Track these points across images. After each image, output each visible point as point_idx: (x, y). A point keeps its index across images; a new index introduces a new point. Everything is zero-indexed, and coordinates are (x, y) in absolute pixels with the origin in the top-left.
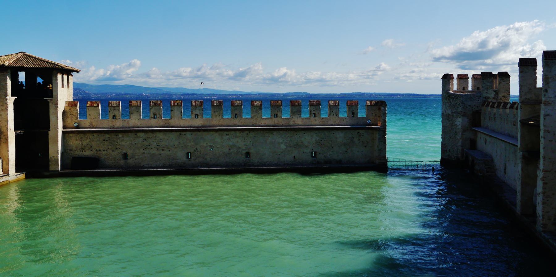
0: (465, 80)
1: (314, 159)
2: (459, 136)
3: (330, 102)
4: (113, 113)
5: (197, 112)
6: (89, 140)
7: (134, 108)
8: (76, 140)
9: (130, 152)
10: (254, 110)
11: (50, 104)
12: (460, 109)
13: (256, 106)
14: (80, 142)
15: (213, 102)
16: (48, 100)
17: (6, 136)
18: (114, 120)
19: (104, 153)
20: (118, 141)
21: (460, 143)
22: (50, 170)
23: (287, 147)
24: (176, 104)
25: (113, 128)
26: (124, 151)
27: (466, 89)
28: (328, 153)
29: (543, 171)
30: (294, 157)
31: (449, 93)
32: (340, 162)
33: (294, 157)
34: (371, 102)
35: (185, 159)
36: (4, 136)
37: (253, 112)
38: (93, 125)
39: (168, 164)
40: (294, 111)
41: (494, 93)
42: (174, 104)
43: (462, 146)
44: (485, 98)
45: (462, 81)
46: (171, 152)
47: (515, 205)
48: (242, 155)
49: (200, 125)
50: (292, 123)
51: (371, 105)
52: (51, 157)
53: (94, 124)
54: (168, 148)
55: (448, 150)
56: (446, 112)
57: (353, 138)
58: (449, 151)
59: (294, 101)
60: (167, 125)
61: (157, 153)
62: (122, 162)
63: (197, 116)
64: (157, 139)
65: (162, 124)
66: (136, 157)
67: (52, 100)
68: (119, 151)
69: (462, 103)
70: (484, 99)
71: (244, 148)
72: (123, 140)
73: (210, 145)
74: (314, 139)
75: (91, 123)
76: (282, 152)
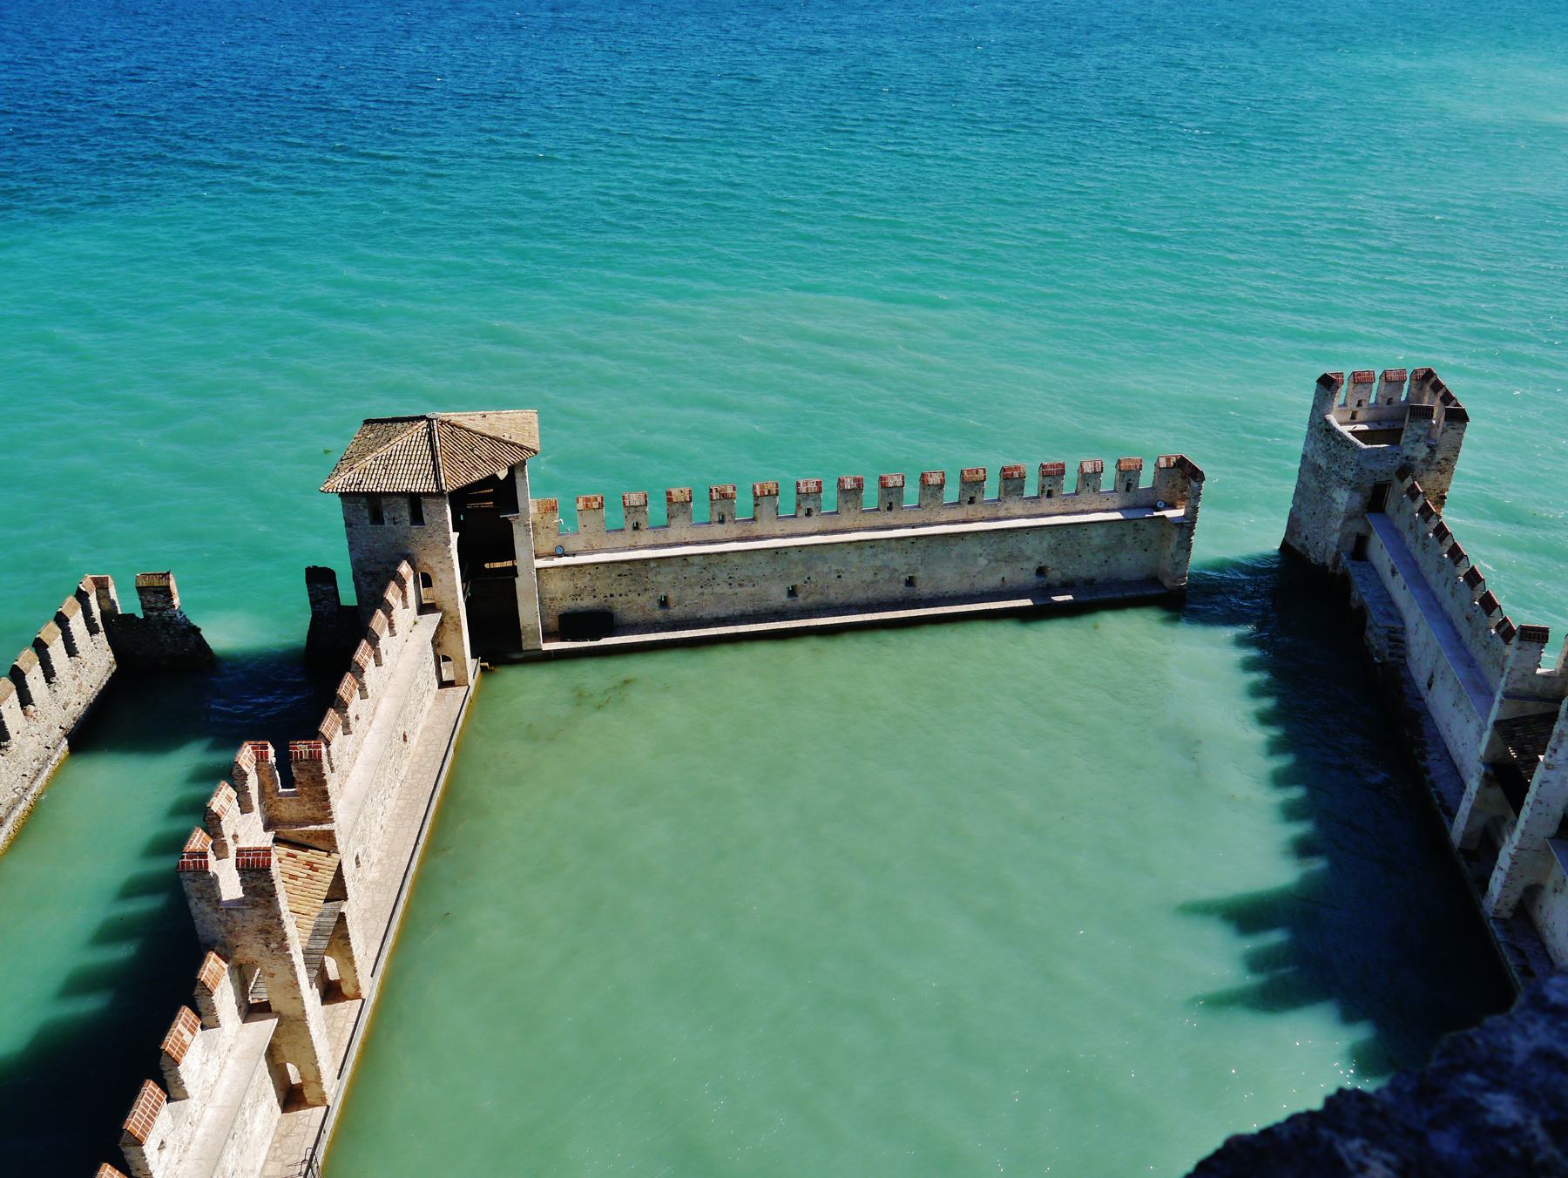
0: (1366, 385)
1: (1040, 580)
2: (1337, 524)
4: (633, 518)
5: (810, 504)
6: (589, 577)
7: (677, 505)
8: (562, 579)
9: (673, 596)
10: (929, 492)
11: (514, 526)
12: (1349, 474)
13: (933, 485)
14: (571, 583)
15: (843, 481)
17: (456, 619)
18: (636, 532)
19: (620, 599)
20: (650, 576)
21: (1335, 537)
23: (990, 561)
24: (766, 493)
25: (634, 548)
26: (663, 593)
27: (1363, 403)
28: (1071, 567)
29: (1515, 848)
31: (1327, 422)
32: (1090, 582)
34: (1168, 460)
35: (784, 598)
36: (452, 618)
37: (922, 495)
38: (591, 545)
39: (751, 609)
40: (1009, 489)
42: (762, 492)
43: (1338, 547)
44: (1407, 458)
45: (1360, 387)
46: (756, 587)
47: (1452, 815)
48: (899, 582)
49: (816, 530)
50: (1002, 513)
52: (524, 627)
53: (594, 543)
54: (750, 580)
55: (1303, 534)
56: (1313, 456)
57: (1124, 535)
58: (1307, 539)
59: (1010, 469)
60: (746, 534)
61: (730, 591)
62: (659, 614)
63: (809, 513)
64: (730, 565)
65: (736, 532)
66: (687, 603)
67: (517, 518)
68: (651, 594)
70: (1404, 461)
71: (904, 569)
72: (656, 575)
73: (836, 568)
74: (1045, 544)
75: (588, 542)
76: (979, 572)
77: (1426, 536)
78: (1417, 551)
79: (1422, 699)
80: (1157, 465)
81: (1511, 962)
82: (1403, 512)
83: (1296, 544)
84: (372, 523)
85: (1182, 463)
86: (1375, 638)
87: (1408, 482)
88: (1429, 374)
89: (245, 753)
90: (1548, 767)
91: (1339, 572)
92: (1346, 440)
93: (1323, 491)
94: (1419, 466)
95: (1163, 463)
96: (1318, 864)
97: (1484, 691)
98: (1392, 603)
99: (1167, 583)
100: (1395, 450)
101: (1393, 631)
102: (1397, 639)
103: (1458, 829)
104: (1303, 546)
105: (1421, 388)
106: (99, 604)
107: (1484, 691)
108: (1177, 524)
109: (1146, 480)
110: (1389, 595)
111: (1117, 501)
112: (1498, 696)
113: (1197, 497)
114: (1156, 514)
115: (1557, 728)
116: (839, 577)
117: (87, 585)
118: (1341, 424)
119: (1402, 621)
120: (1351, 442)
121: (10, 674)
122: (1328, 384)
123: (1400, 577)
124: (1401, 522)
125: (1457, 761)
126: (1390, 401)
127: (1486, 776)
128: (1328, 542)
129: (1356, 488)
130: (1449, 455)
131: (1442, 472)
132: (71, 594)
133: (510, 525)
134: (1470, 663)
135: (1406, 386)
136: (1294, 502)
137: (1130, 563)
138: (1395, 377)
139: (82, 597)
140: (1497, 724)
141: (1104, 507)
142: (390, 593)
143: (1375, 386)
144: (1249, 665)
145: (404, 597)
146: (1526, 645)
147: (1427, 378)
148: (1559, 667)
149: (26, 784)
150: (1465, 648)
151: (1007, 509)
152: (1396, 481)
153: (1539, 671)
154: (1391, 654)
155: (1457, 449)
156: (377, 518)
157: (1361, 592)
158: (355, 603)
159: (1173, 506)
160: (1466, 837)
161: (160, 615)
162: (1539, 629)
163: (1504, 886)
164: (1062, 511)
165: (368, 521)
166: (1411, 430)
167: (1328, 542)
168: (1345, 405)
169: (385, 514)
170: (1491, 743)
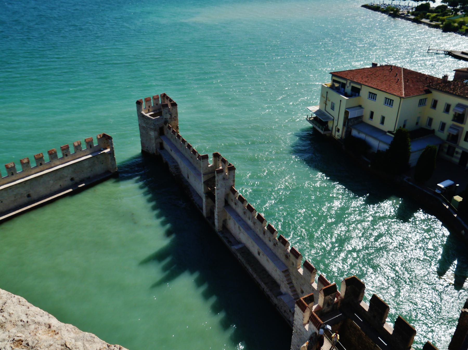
2: (153, 141)
3: (75, 144)
12: (152, 127)
21: (154, 145)
30: (60, 185)
31: (142, 114)
32: (89, 178)
33: (60, 185)
34: (100, 135)
37: (23, 167)
41: (170, 115)
44: (165, 119)
45: (148, 102)
47: (202, 209)
50: (53, 165)
51: (101, 138)
55: (146, 146)
57: (94, 161)
59: (50, 151)
69: (153, 124)
77: (176, 138)
78: (174, 143)
79: (188, 182)
80: (97, 138)
81: (225, 241)
82: (168, 134)
83: (145, 150)
85: (104, 135)
86: (172, 169)
87: (167, 125)
88: (164, 95)
90: (217, 189)
91: (158, 154)
92: (148, 118)
93: (147, 133)
94: (169, 120)
95: (99, 137)
96: (173, 236)
97: (199, 175)
98: (173, 159)
99: (112, 171)
100: (162, 117)
101: (175, 166)
102: (177, 168)
103: (204, 212)
104: (147, 150)
105: (164, 99)
107: (199, 175)
108: (109, 154)
109: (95, 144)
110: (172, 157)
111: (89, 152)
112: (202, 175)
113: (112, 144)
114: (102, 152)
115: (216, 180)
116: (2, 202)
118: (146, 113)
119: (177, 162)
120: (150, 118)
122: (139, 103)
123: (173, 151)
124: (169, 136)
125: (200, 195)
126: (157, 104)
127: (206, 197)
128: (153, 147)
129: (155, 130)
130: (176, 115)
131: (175, 120)
134: (195, 169)
135: (160, 99)
136: (141, 138)
137: (99, 169)
138: (156, 97)
140: (204, 182)
141: (85, 154)
143: (152, 101)
144: (141, 188)
146: (204, 160)
147: (164, 96)
148: (213, 163)
150: (193, 165)
151: (54, 164)
152: (165, 126)
153: (209, 166)
154: (177, 172)
155: (177, 113)
157: (165, 158)
159: (106, 149)
160: (207, 214)
162: (206, 155)
163: (218, 223)
164: (72, 159)
166: (164, 111)
167: (153, 147)
168: (145, 108)
170: (204, 188)
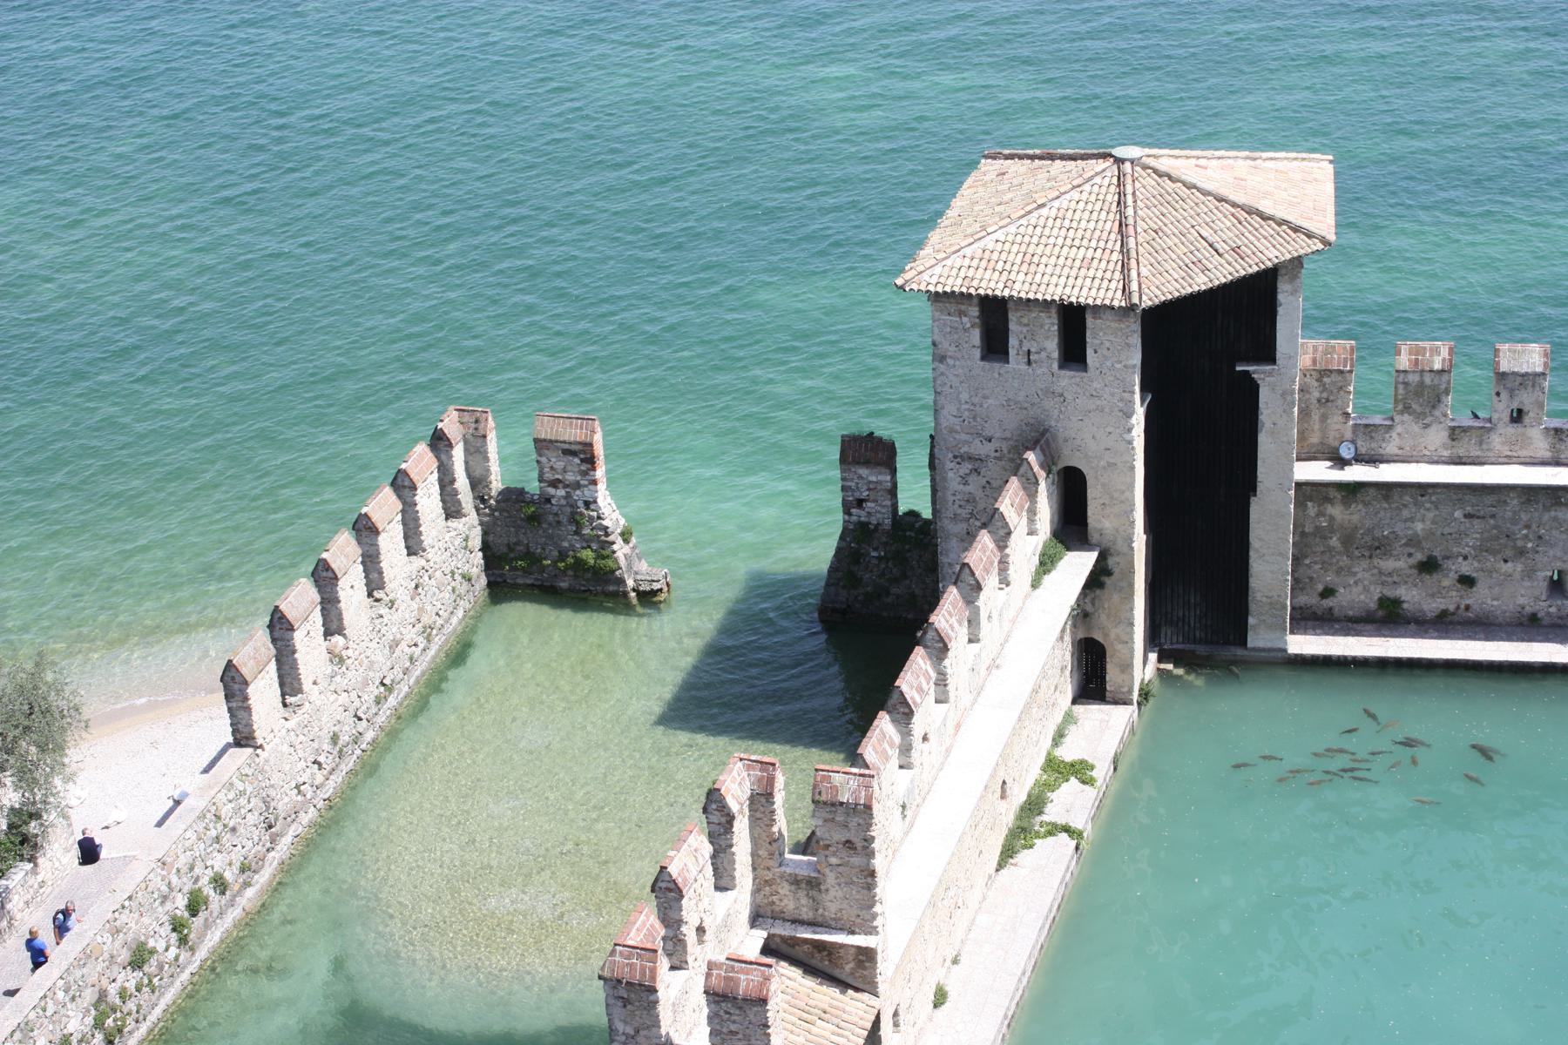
16: (1255, 376)
22: (1250, 644)
67: (1270, 374)
84: (983, 358)
89: (735, 773)
106: (466, 463)
117: (451, 425)
121: (313, 574)
132: (422, 438)
133: (1250, 389)
139: (439, 442)
142: (1007, 501)
145: (1032, 512)
149: (319, 778)
156: (995, 345)
158: (930, 517)
161: (568, 496)
165: (977, 353)
169: (1013, 342)
